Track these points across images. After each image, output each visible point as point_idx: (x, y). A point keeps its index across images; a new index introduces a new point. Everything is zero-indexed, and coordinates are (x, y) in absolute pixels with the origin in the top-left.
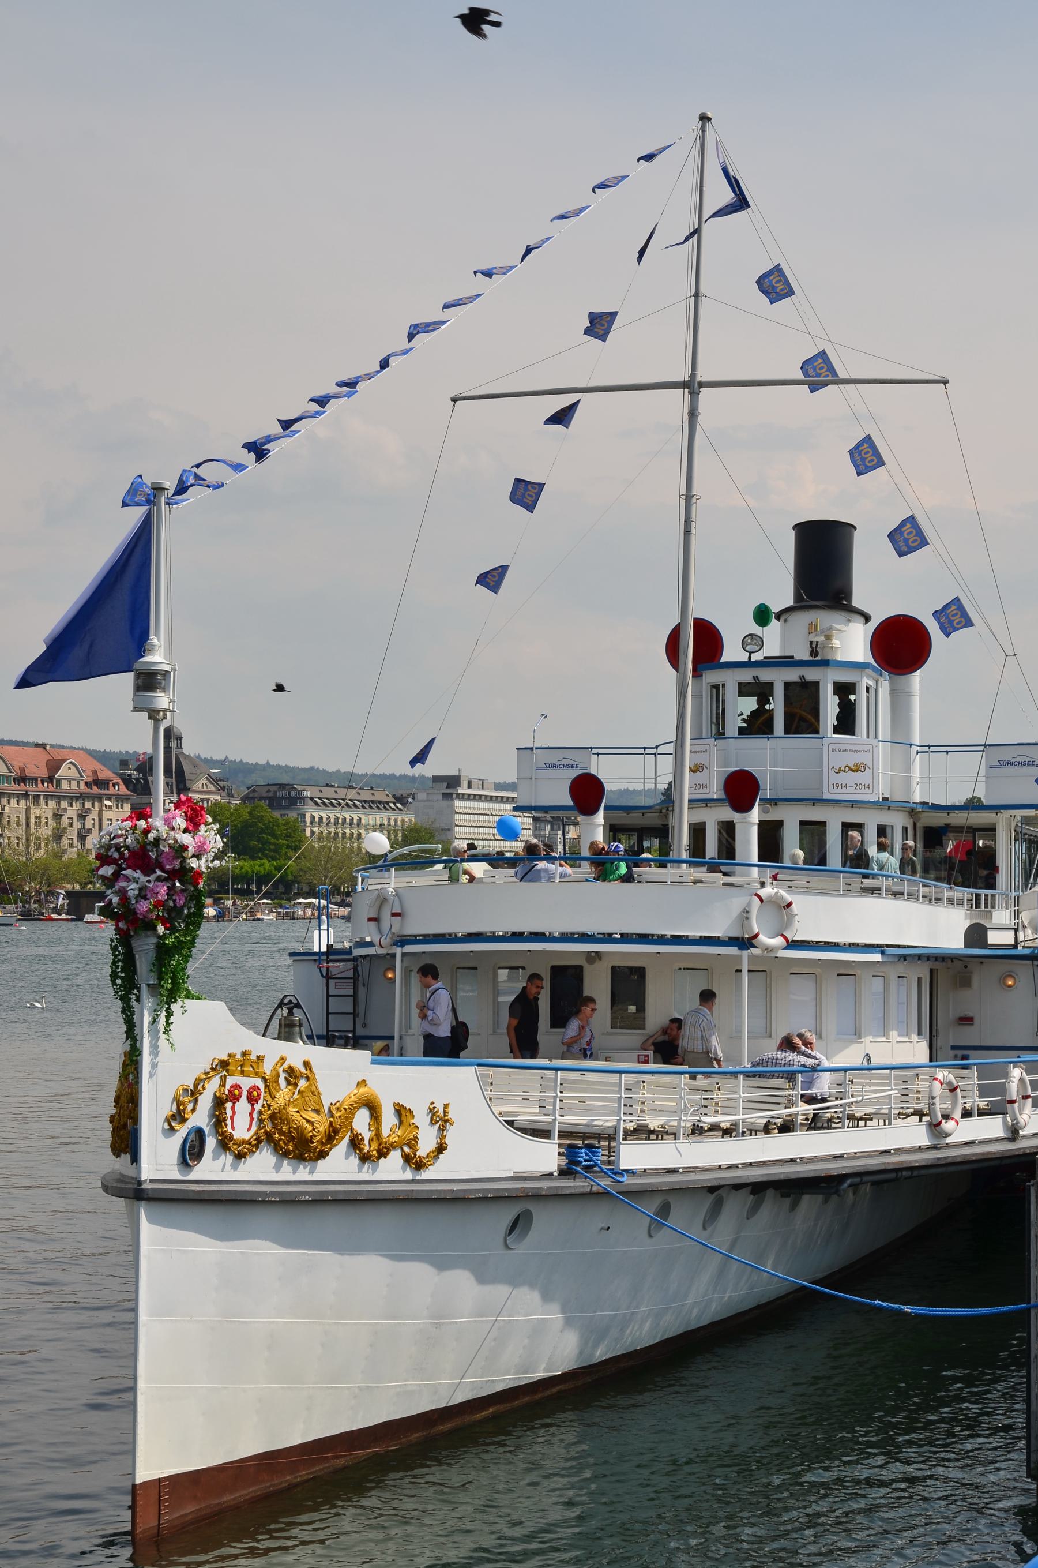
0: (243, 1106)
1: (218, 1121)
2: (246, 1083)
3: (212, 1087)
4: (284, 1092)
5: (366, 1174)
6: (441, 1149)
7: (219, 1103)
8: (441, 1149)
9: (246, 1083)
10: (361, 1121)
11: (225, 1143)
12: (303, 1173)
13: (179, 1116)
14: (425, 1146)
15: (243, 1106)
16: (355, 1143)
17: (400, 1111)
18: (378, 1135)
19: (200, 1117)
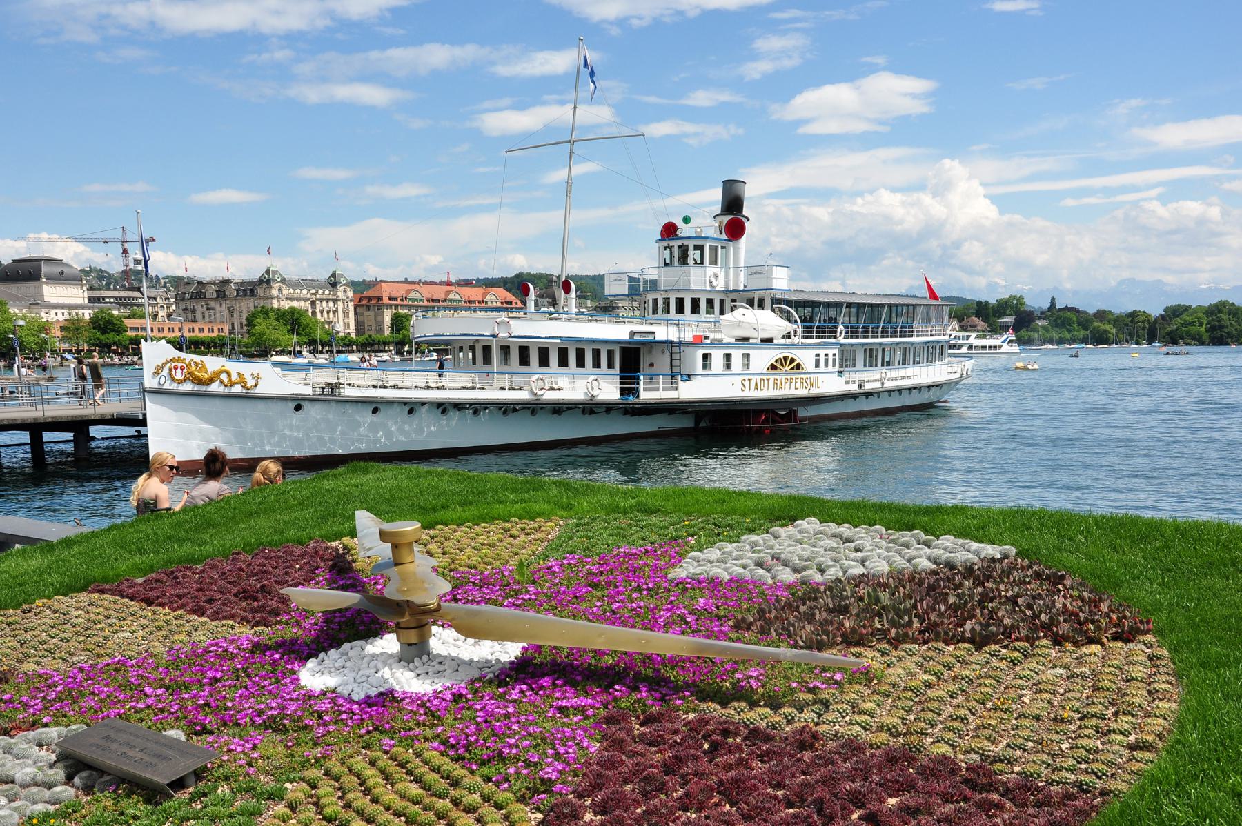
0: (179, 371)
1: (171, 374)
2: (179, 365)
3: (168, 366)
4: (193, 367)
5: (227, 390)
6: (256, 385)
7: (170, 370)
8: (256, 385)
9: (179, 365)
10: (224, 377)
11: (173, 379)
12: (203, 389)
13: (156, 373)
14: (251, 383)
15: (179, 371)
16: (222, 382)
17: (239, 374)
18: (230, 380)
19: (165, 371)
